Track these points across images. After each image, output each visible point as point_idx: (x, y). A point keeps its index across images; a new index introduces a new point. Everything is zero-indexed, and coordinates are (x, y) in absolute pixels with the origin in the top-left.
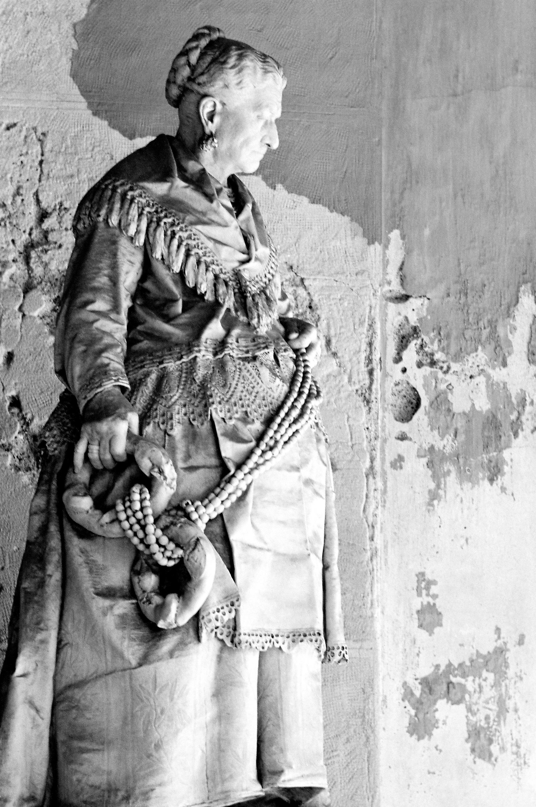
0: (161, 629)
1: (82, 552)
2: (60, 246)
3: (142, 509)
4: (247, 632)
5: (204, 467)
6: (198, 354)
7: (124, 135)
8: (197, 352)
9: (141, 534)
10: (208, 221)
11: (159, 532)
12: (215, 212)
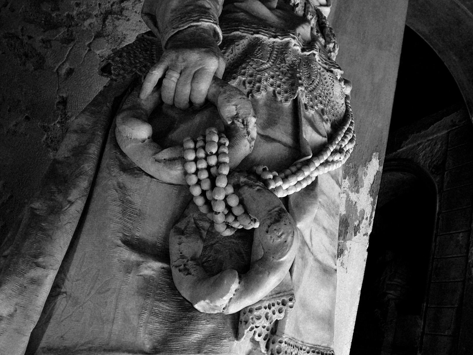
0: (196, 310)
1: (120, 187)
2: (128, 20)
3: (217, 154)
5: (279, 142)
9: (206, 186)
11: (230, 190)
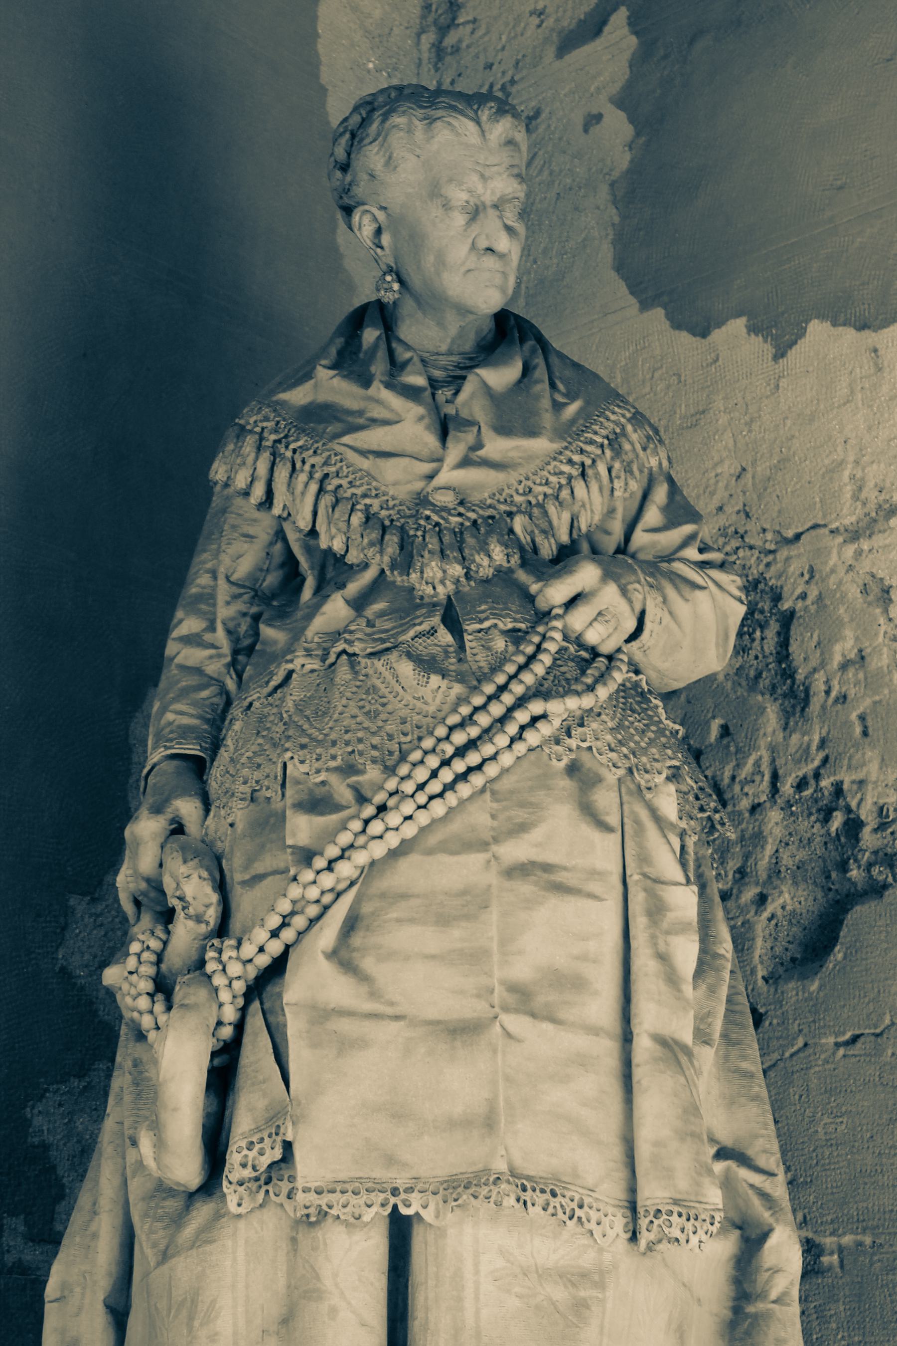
4: (313, 1185)
6: (290, 666)
7: (694, 335)
8: (288, 662)
10: (367, 423)
12: (378, 401)
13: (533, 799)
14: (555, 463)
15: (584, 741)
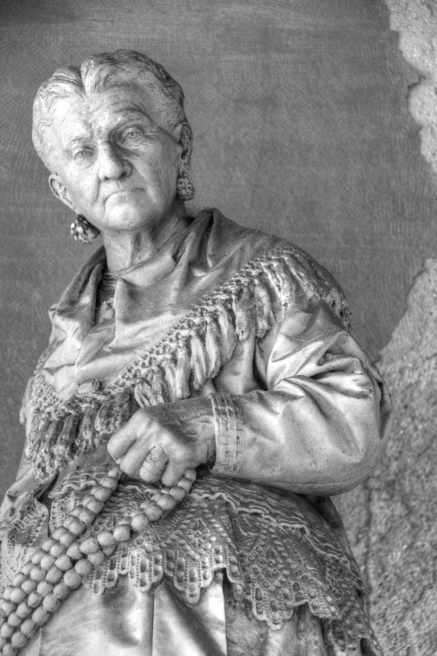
13: (73, 633)
14: (178, 331)
15: (123, 569)
